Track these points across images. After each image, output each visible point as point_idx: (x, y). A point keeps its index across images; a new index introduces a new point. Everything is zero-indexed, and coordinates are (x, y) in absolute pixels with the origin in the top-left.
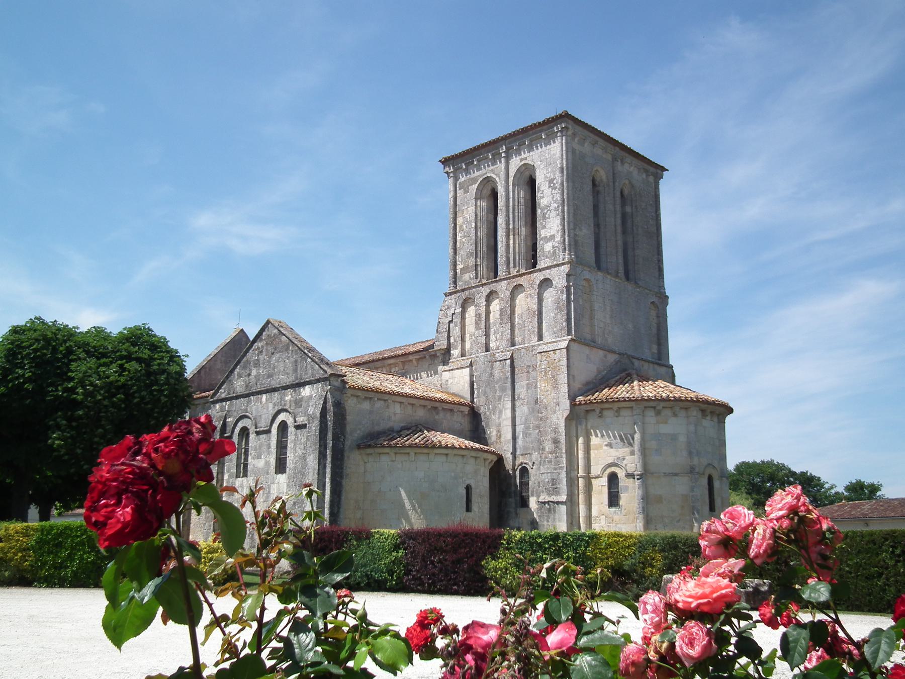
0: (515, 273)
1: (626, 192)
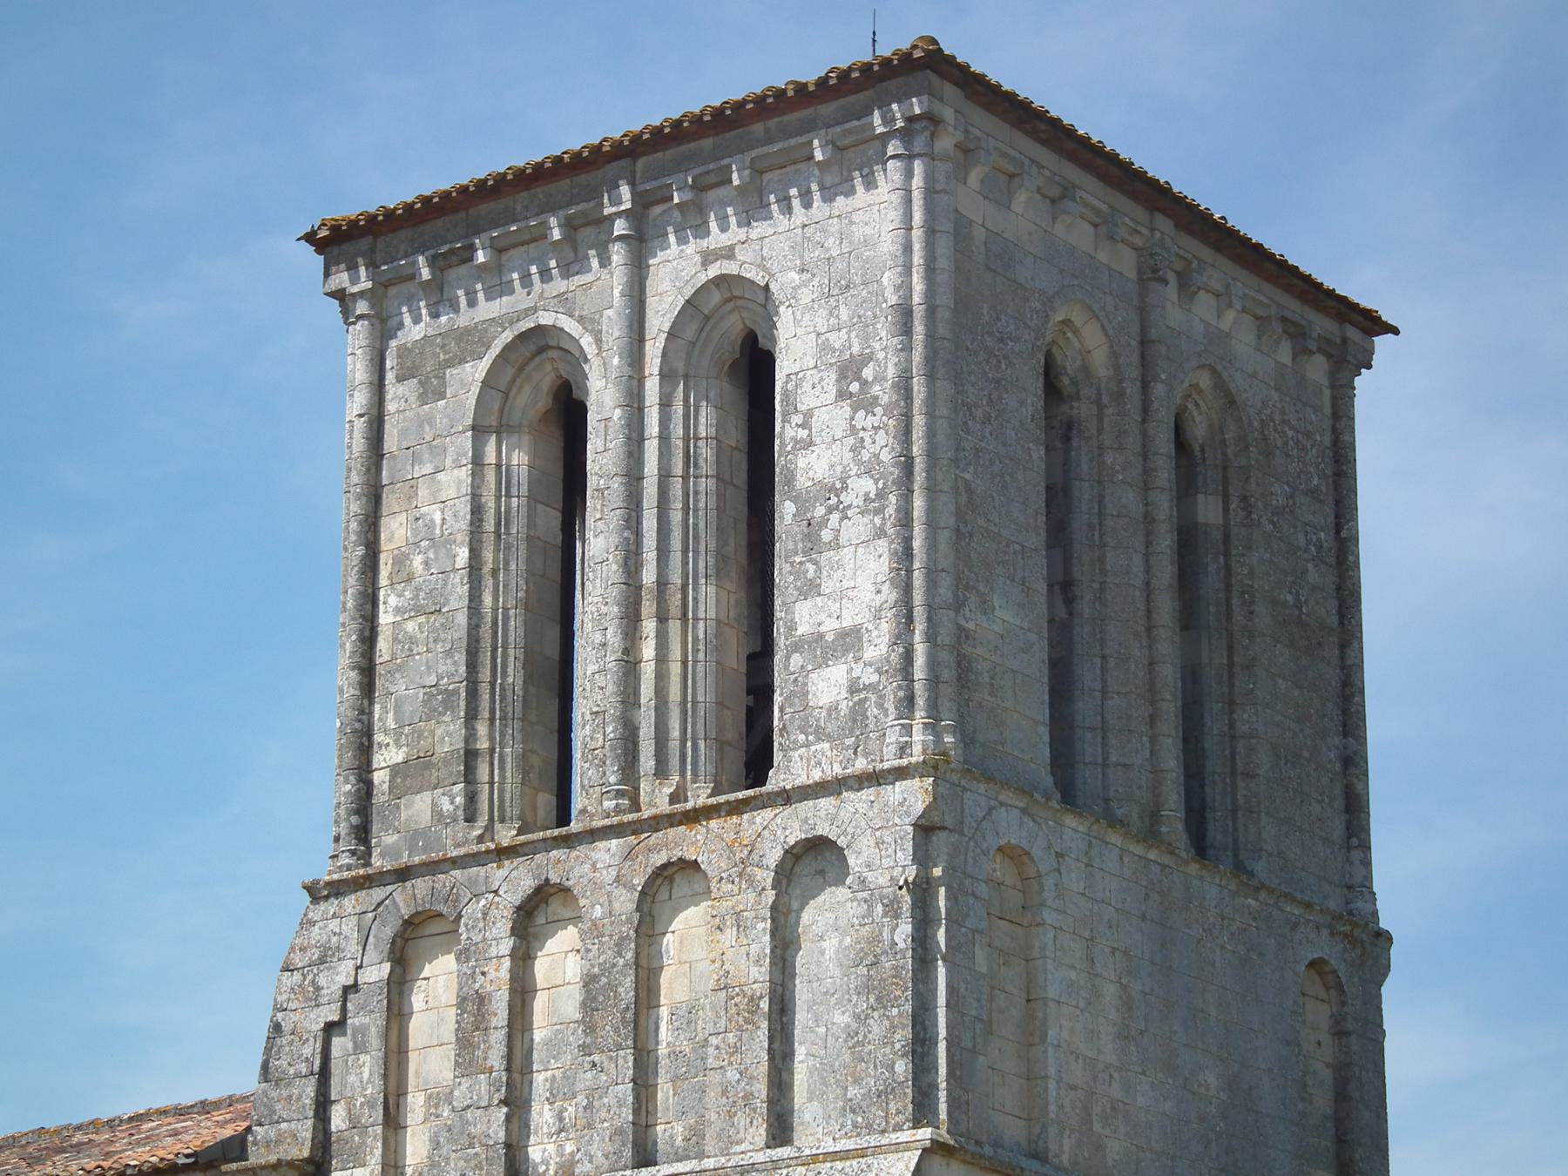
0: (663, 806)
1: (1199, 430)
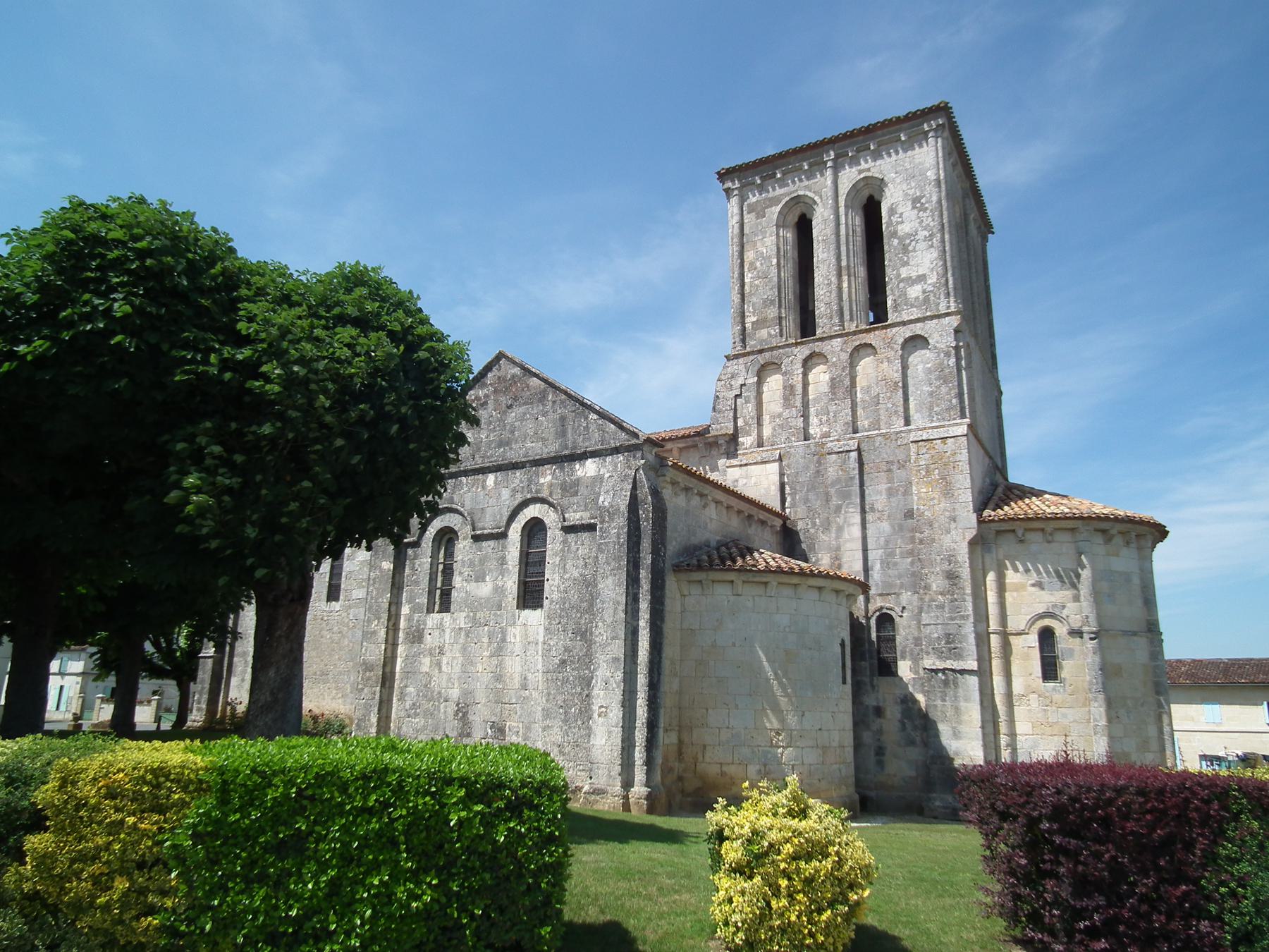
0: (853, 328)
